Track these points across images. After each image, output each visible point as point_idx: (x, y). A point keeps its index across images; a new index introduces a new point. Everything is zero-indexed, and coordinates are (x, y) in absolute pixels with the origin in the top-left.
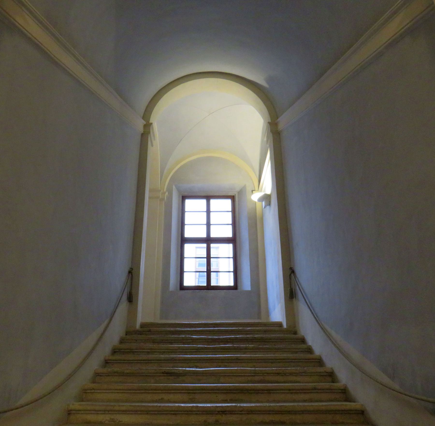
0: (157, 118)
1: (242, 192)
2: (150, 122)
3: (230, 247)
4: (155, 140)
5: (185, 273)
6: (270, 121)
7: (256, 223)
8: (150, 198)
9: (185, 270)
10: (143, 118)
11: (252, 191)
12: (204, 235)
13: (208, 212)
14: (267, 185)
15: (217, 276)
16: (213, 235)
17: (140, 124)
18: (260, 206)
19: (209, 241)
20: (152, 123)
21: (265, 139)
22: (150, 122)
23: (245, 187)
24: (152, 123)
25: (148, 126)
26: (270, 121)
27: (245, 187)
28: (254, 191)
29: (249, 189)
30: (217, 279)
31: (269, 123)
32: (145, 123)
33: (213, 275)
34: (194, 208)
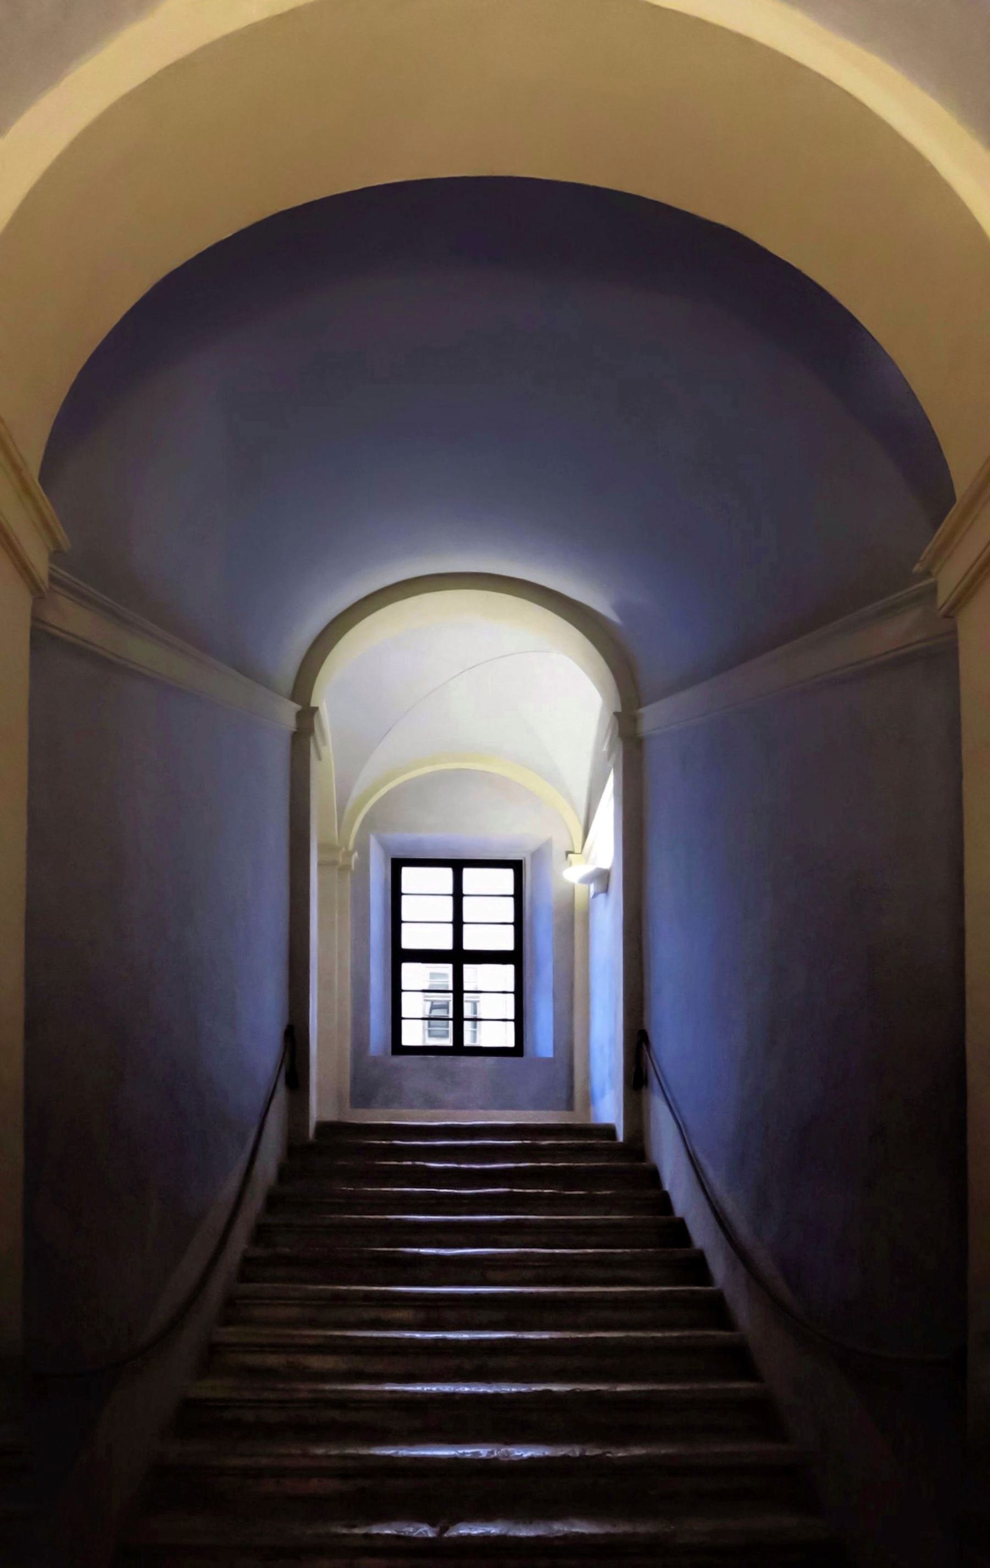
0: (327, 696)
1: (540, 854)
2: (313, 704)
3: (508, 971)
4: (325, 743)
5: (403, 897)
6: (619, 710)
7: (572, 922)
8: (319, 865)
9: (404, 889)
10: (293, 698)
11: (568, 853)
12: (447, 944)
13: (458, 896)
14: (604, 847)
15: (475, 1027)
16: (469, 944)
17: (288, 712)
18: (584, 891)
19: (458, 957)
20: (316, 709)
21: (605, 749)
22: (313, 704)
23: (548, 843)
24: (316, 709)
25: (307, 715)
26: (619, 710)
27: (548, 843)
28: (572, 852)
29: (558, 849)
30: (475, 1032)
31: (616, 714)
32: (298, 707)
33: (467, 1025)
34: (425, 891)
